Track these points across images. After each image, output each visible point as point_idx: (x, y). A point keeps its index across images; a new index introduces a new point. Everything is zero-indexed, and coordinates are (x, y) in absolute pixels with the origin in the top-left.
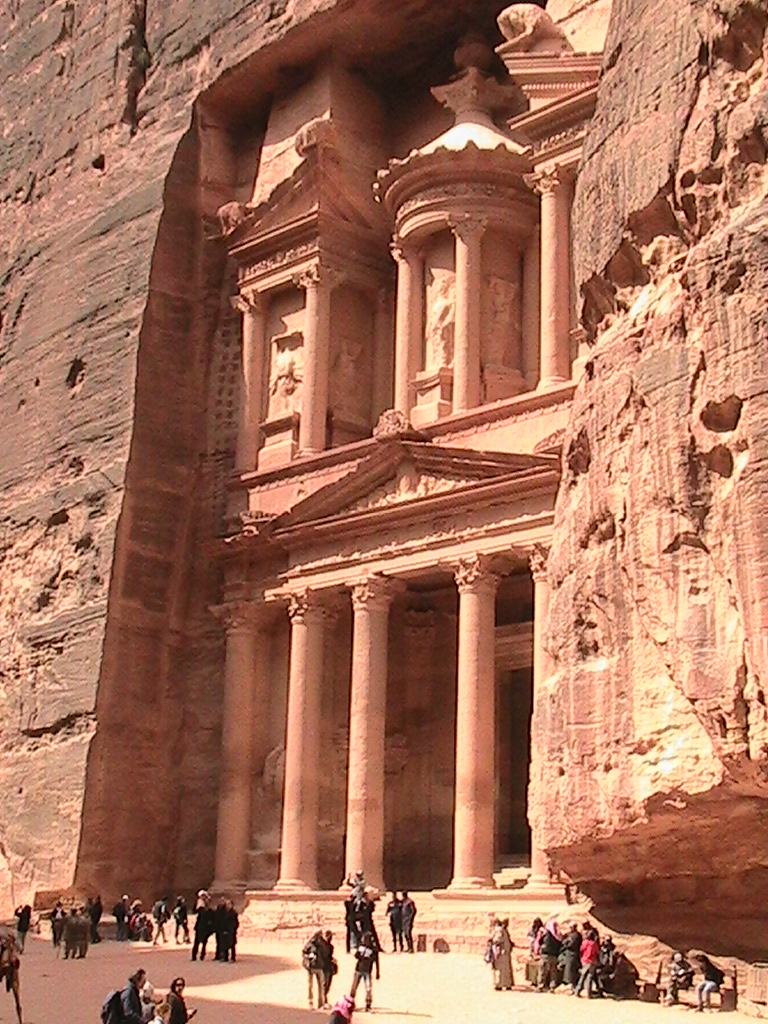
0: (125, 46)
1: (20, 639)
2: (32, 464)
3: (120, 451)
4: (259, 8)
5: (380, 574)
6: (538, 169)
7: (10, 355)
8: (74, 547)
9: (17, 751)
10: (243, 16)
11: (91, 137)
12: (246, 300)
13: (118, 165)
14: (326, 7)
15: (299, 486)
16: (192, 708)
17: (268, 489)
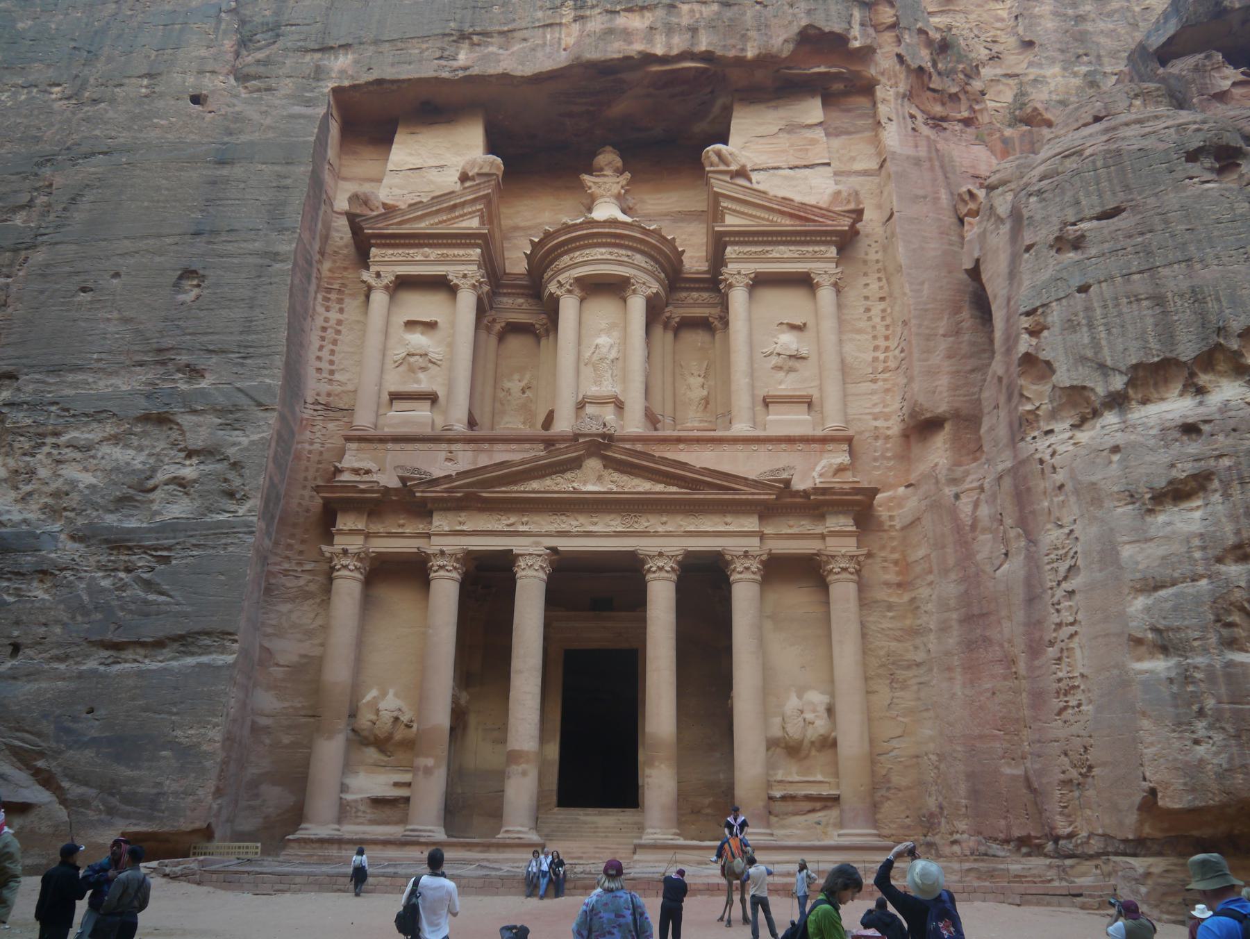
0: (229, 11)
1: (73, 538)
2: (103, 356)
3: (266, 372)
4: (424, 46)
5: (554, 550)
6: (730, 266)
7: (58, 237)
8: (183, 454)
9: (77, 663)
10: (400, 45)
11: (185, 73)
12: (378, 275)
13: (231, 110)
14: (519, 73)
15: (443, 455)
16: (267, 645)
17: (402, 450)
